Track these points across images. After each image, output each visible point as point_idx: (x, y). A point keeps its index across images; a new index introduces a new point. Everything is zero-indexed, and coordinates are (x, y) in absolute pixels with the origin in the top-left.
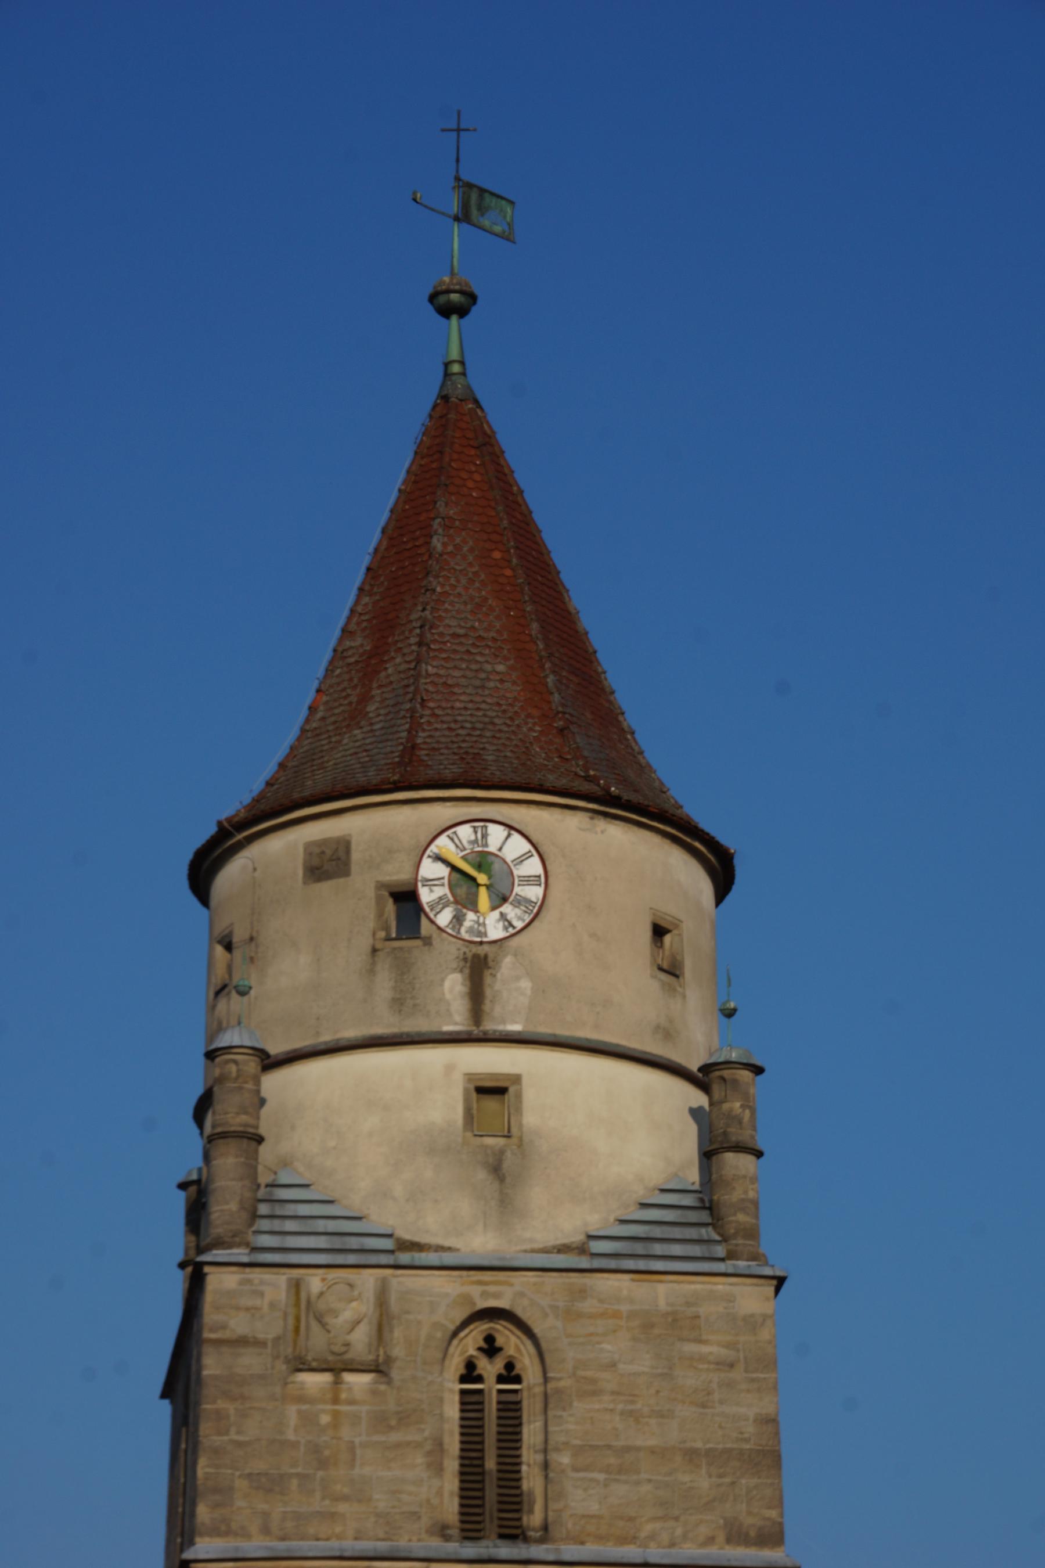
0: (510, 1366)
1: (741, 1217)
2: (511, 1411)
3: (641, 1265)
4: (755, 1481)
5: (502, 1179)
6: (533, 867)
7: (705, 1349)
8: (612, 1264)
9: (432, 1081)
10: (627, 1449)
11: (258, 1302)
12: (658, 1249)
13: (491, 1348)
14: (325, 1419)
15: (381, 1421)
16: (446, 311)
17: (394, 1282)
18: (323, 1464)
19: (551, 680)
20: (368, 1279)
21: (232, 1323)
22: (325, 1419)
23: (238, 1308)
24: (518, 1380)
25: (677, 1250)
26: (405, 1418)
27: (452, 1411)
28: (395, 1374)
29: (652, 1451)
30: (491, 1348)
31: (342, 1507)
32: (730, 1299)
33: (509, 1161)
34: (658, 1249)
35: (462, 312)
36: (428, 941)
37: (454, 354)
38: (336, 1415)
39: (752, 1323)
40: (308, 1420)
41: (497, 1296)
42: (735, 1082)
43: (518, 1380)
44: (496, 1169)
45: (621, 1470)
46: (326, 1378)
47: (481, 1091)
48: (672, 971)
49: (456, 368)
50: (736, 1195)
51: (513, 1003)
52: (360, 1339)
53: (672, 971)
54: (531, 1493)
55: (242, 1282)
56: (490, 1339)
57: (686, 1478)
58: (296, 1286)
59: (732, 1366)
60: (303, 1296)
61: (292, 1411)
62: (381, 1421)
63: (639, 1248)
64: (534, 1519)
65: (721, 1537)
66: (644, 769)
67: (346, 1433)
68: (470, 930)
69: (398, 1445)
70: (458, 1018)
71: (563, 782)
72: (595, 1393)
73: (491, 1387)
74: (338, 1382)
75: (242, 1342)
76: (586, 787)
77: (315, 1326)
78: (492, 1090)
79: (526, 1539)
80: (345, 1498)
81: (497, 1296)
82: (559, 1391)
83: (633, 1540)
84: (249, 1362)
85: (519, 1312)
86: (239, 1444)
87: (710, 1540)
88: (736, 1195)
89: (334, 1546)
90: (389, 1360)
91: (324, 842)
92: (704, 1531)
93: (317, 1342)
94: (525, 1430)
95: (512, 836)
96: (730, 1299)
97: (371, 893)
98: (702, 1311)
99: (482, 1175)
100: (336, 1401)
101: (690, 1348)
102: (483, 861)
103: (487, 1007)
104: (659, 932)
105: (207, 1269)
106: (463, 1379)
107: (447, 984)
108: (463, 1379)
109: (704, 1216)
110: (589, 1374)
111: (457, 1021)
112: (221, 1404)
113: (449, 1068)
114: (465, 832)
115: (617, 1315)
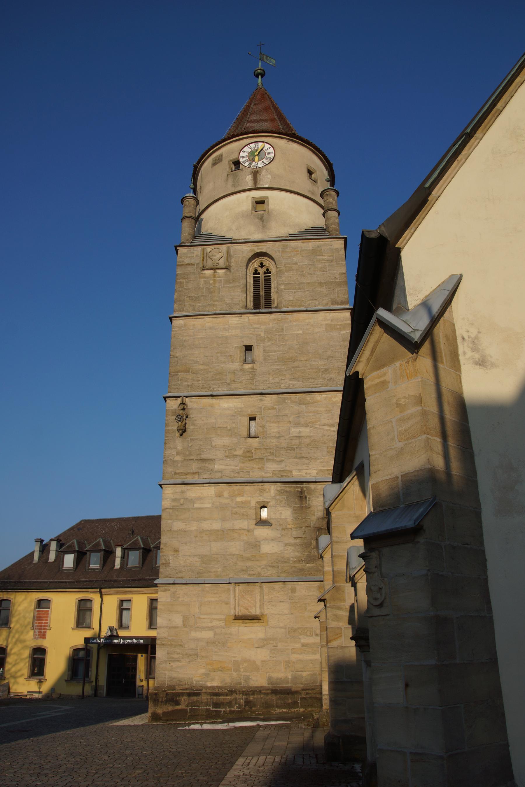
0: (267, 270)
2: (268, 282)
4: (339, 289)
5: (263, 221)
6: (272, 150)
7: (324, 257)
9: (244, 201)
10: (301, 283)
11: (193, 255)
13: (262, 265)
14: (211, 282)
15: (228, 281)
17: (232, 248)
18: (211, 293)
19: (279, 124)
20: (224, 247)
21: (185, 261)
22: (211, 282)
23: (187, 257)
24: (270, 273)
26: (234, 281)
27: (250, 281)
28: (232, 270)
29: (308, 283)
30: (262, 265)
31: (216, 303)
32: (331, 245)
33: (265, 217)
36: (242, 170)
38: (214, 281)
39: (337, 250)
40: (206, 282)
41: (261, 249)
42: (330, 194)
43: (270, 273)
44: (261, 219)
45: (299, 289)
46: (212, 271)
48: (315, 181)
51: (265, 180)
52: (222, 263)
53: (315, 181)
54: (274, 299)
55: (188, 251)
57: (319, 289)
58: (204, 250)
59: (332, 261)
60: (205, 252)
61: (202, 281)
62: (228, 281)
65: (330, 303)
67: (217, 285)
68: (254, 166)
69: (233, 287)
70: (250, 185)
72: (291, 270)
73: (262, 276)
74: (215, 273)
75: (188, 265)
77: (208, 259)
78: (260, 202)
80: (217, 301)
81: (261, 249)
82: (280, 270)
84: (190, 269)
85: (268, 252)
86: (186, 289)
87: (327, 304)
89: (213, 312)
90: (230, 266)
91: (217, 157)
92: (324, 302)
93: (209, 264)
94: (272, 285)
96: (331, 245)
97: (227, 163)
98: (322, 248)
99: (257, 220)
100: (215, 277)
101: (319, 258)
103: (258, 182)
105: (178, 248)
106: (254, 274)
107: (247, 178)
108: (254, 274)
110: (289, 266)
111: (250, 185)
112: (181, 280)
113: (248, 197)
114: (252, 145)
115: (297, 251)
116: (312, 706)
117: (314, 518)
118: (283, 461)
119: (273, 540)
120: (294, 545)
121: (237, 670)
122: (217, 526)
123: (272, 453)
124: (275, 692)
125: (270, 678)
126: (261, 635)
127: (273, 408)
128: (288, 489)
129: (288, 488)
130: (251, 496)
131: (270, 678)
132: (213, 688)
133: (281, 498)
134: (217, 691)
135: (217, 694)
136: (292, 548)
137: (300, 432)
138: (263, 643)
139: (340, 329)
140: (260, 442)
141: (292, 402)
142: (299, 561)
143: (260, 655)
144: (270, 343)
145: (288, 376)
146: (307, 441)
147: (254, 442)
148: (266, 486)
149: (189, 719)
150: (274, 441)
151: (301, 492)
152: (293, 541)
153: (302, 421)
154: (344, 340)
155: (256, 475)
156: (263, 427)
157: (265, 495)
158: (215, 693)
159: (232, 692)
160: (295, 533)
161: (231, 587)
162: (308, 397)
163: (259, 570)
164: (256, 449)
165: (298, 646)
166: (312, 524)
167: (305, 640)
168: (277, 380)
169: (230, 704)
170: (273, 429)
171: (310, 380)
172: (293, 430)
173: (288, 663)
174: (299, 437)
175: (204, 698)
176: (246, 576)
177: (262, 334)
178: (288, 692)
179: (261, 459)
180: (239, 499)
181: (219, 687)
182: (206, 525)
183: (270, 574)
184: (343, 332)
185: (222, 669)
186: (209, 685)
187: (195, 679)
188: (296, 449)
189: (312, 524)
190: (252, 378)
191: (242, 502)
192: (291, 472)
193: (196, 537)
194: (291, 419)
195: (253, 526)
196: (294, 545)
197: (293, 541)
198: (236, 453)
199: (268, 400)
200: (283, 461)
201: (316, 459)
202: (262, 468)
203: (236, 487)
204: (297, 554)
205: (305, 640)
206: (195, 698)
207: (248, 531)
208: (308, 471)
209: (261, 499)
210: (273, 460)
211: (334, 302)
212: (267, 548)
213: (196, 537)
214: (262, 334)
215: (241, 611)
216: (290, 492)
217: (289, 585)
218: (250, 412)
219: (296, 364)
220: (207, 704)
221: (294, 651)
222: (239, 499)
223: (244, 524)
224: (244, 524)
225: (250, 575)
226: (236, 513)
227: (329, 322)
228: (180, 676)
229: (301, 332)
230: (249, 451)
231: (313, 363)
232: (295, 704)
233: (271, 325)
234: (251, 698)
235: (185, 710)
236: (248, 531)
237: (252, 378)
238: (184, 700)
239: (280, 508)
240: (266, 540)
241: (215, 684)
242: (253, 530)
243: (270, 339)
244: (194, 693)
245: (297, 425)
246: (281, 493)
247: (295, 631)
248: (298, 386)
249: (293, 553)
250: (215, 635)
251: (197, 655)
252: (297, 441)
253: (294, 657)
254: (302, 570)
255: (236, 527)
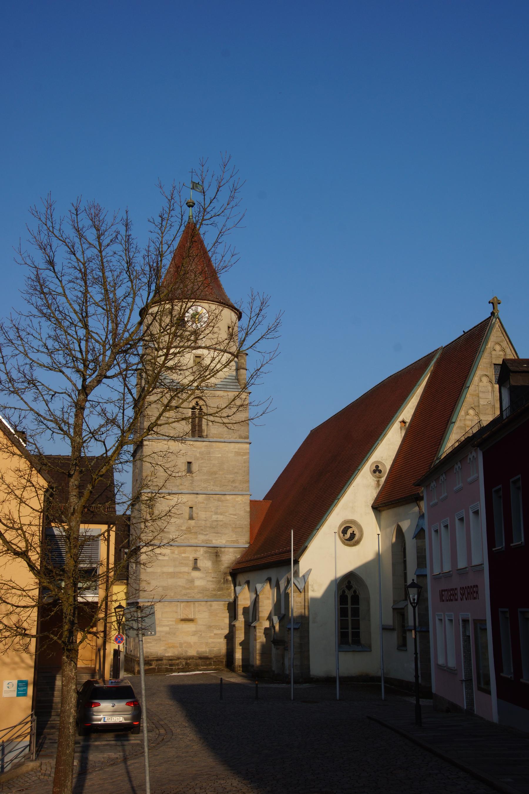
1: (243, 381)
3: (225, 390)
8: (220, 389)
12: (228, 387)
13: (197, 404)
16: (189, 206)
25: (231, 387)
30: (197, 404)
34: (228, 387)
35: (192, 206)
37: (191, 215)
47: (196, 357)
49: (191, 217)
50: (242, 377)
56: (197, 402)
63: (225, 386)
64: (205, 434)
66: (226, 296)
71: (212, 299)
76: (217, 300)
79: (203, 437)
83: (222, 438)
87: (236, 438)
88: (242, 377)
92: (235, 436)
95: (203, 308)
102: (197, 313)
104: (229, 327)
109: (236, 381)
116: (219, 665)
117: (223, 567)
118: (207, 534)
119: (201, 578)
120: (212, 581)
121: (181, 647)
122: (171, 570)
123: (202, 530)
124: (200, 658)
125: (198, 651)
126: (194, 629)
127: (203, 503)
128: (210, 551)
129: (210, 550)
130: (190, 554)
131: (198, 651)
132: (168, 656)
133: (206, 555)
134: (171, 658)
135: (171, 660)
136: (211, 583)
137: (217, 518)
138: (195, 633)
139: (243, 455)
140: (195, 523)
141: (214, 499)
142: (214, 590)
143: (193, 640)
144: (202, 461)
145: (212, 483)
146: (221, 523)
147: (192, 522)
148: (198, 548)
149: (157, 673)
150: (203, 522)
151: (217, 553)
152: (211, 579)
153: (219, 511)
154: (244, 463)
155: (193, 542)
156: (197, 514)
157: (198, 553)
158: (170, 659)
159: (179, 658)
160: (213, 575)
161: (179, 603)
162: (223, 497)
163: (193, 594)
164: (193, 527)
165: (212, 635)
166: (222, 570)
167: (216, 632)
168: (205, 485)
169: (178, 665)
170: (202, 515)
171: (224, 487)
172: (214, 516)
173: (207, 644)
174: (217, 521)
175: (164, 662)
176: (187, 598)
177: (198, 455)
178: (206, 658)
179: (196, 533)
180: (183, 555)
181: (172, 656)
182: (165, 570)
183: (199, 596)
184: (244, 457)
185: (174, 647)
186: (167, 655)
187: (160, 652)
188: (215, 528)
189: (222, 570)
190: (192, 483)
191: (185, 557)
192: (211, 541)
193: (160, 576)
194: (213, 510)
195: (190, 571)
196: (212, 581)
197: (211, 579)
198: (182, 528)
199: (201, 498)
200: (207, 534)
201: (225, 534)
202: (196, 538)
203: (182, 548)
204: (213, 586)
205: (216, 632)
206: (160, 662)
207: (188, 573)
208: (221, 541)
209: (195, 556)
210: (202, 534)
211: (241, 437)
212: (198, 583)
213: (160, 576)
214: (198, 455)
215: (184, 617)
216: (211, 552)
217: (209, 603)
218: (190, 504)
219: (217, 476)
220: (166, 665)
221: (210, 637)
222: (183, 555)
223: (186, 569)
224: (186, 569)
225: (188, 597)
226: (182, 563)
227: (237, 450)
228: (152, 651)
229: (220, 455)
230: (190, 528)
231: (226, 476)
232: (210, 664)
233: (203, 449)
234: (189, 661)
235: (154, 669)
236: (188, 573)
237: (192, 483)
238: (154, 663)
239: (205, 561)
240: (197, 578)
241: (170, 654)
242: (191, 573)
243: (202, 459)
244: (160, 659)
245: (216, 513)
246: (206, 552)
247: (210, 627)
248: (217, 490)
249: (211, 586)
250: (170, 629)
251: (160, 639)
252: (215, 523)
253: (210, 641)
254: (215, 595)
255: (182, 571)
